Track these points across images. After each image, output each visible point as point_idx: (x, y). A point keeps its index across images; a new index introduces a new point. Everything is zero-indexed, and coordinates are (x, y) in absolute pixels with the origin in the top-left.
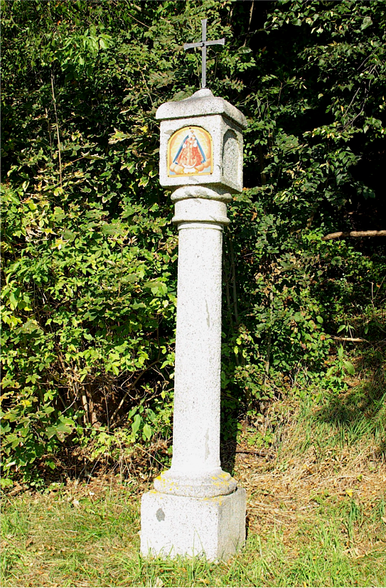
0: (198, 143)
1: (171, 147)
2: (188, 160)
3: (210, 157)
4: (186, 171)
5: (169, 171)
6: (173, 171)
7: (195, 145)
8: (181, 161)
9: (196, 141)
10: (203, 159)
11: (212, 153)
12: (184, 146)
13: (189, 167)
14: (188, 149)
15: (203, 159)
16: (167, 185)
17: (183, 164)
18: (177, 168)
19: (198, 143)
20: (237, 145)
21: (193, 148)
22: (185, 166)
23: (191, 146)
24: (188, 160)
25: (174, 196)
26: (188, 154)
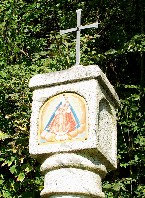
0: (72, 109)
1: (43, 115)
2: (61, 127)
3: (84, 122)
4: (58, 138)
5: (39, 138)
6: (44, 138)
7: (69, 111)
8: (53, 128)
9: (69, 107)
10: (77, 125)
11: (87, 118)
12: (57, 113)
13: (62, 133)
14: (61, 116)
15: (77, 125)
16: (37, 153)
17: (55, 132)
18: (48, 136)
19: (72, 109)
20: (111, 119)
21: (67, 114)
22: (57, 133)
23: (64, 113)
24: (61, 127)
25: (44, 166)
26: (61, 121)
